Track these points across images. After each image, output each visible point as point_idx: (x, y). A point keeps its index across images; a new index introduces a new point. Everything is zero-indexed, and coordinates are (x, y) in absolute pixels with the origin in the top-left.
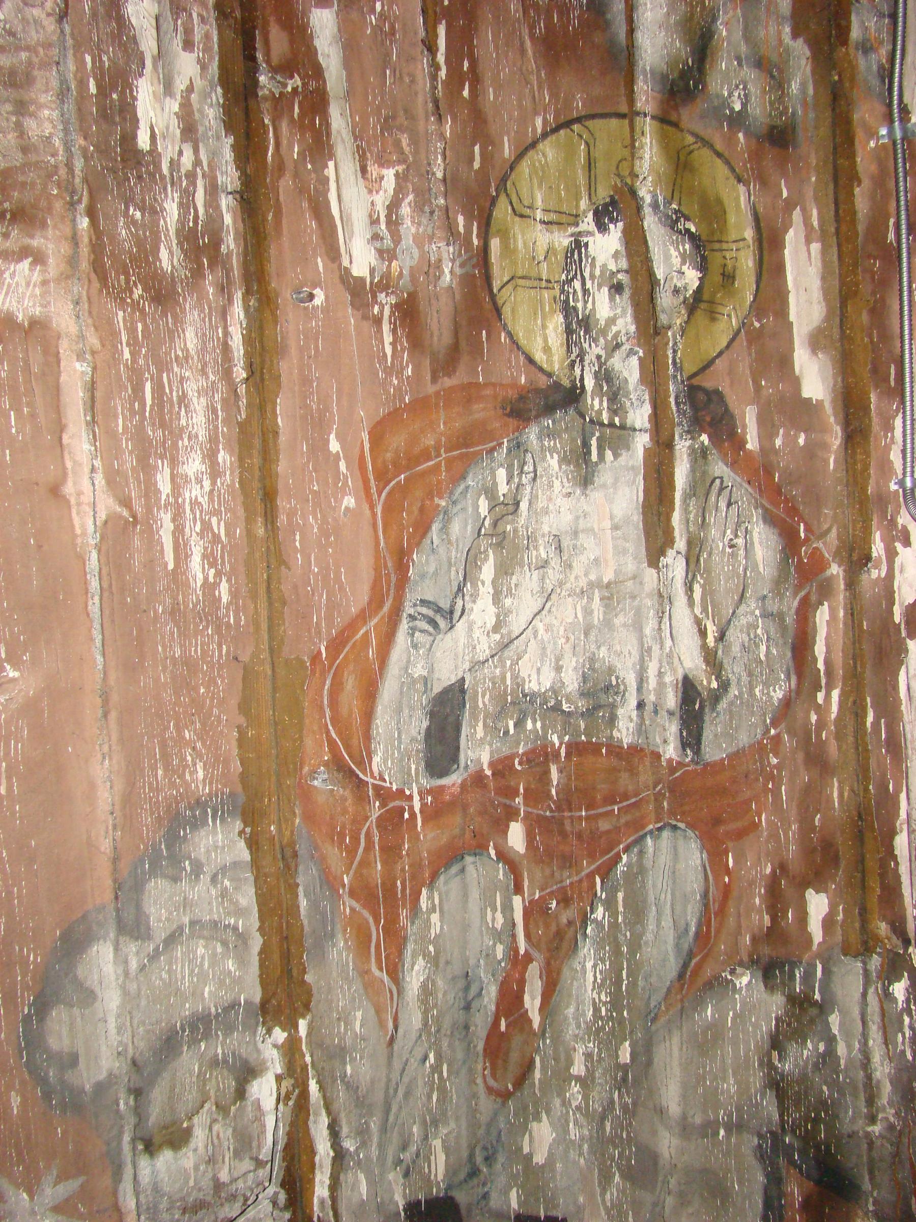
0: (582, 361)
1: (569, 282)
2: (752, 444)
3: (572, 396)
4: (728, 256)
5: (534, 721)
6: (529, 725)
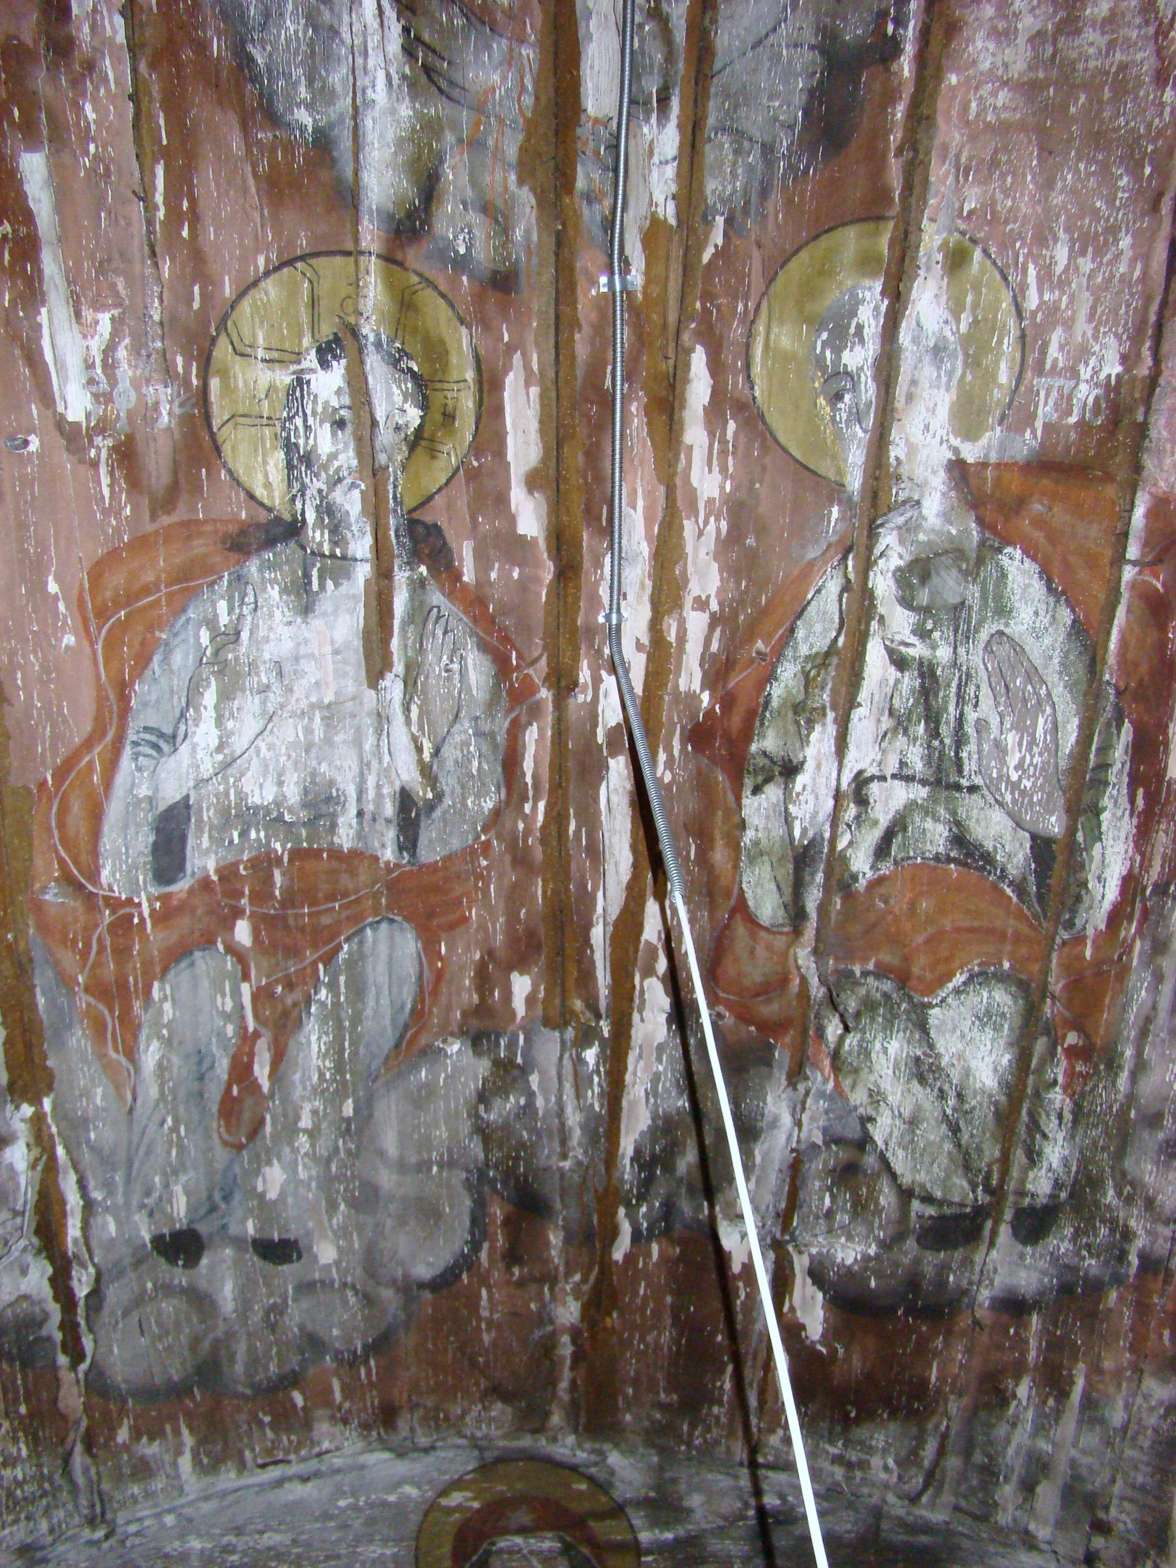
0: (303, 495)
1: (290, 419)
2: (468, 576)
3: (293, 529)
4: (449, 395)
5: (258, 832)
6: (253, 835)
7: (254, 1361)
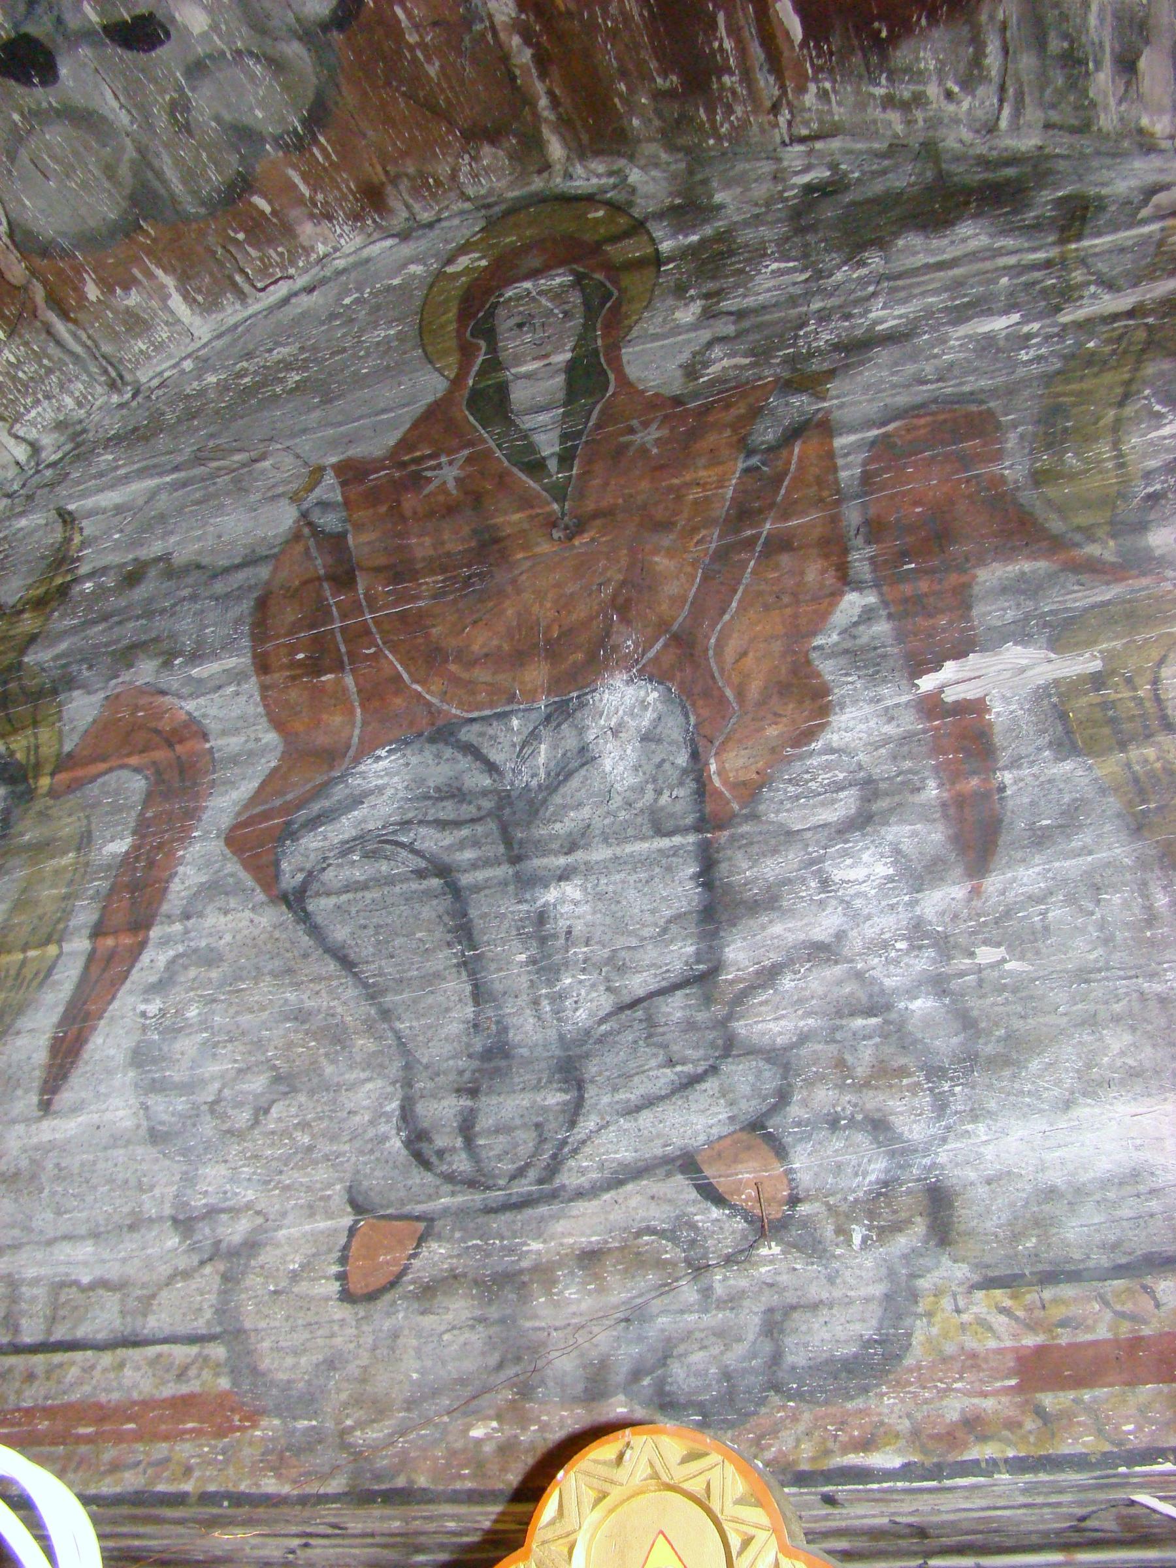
7: (189, 176)
